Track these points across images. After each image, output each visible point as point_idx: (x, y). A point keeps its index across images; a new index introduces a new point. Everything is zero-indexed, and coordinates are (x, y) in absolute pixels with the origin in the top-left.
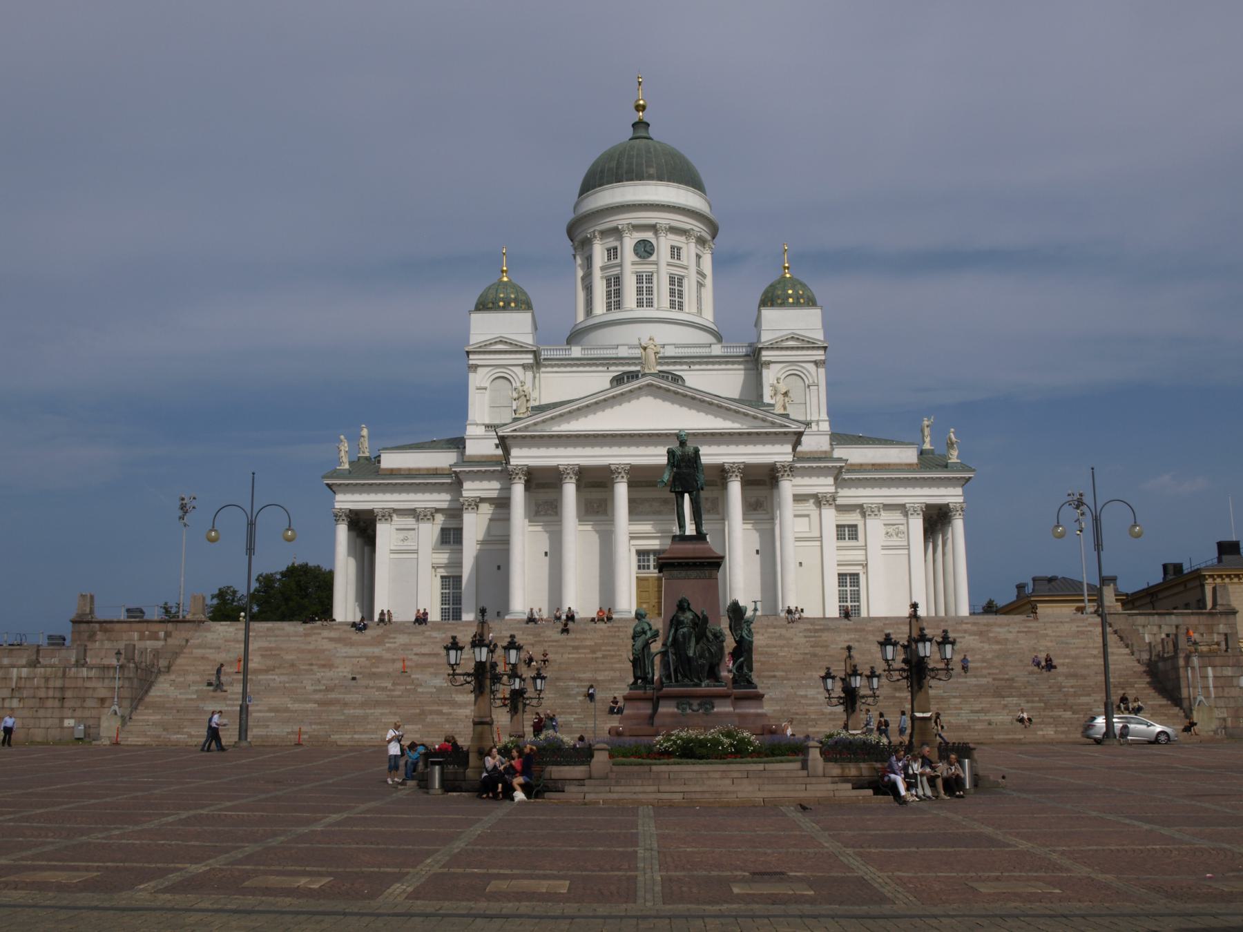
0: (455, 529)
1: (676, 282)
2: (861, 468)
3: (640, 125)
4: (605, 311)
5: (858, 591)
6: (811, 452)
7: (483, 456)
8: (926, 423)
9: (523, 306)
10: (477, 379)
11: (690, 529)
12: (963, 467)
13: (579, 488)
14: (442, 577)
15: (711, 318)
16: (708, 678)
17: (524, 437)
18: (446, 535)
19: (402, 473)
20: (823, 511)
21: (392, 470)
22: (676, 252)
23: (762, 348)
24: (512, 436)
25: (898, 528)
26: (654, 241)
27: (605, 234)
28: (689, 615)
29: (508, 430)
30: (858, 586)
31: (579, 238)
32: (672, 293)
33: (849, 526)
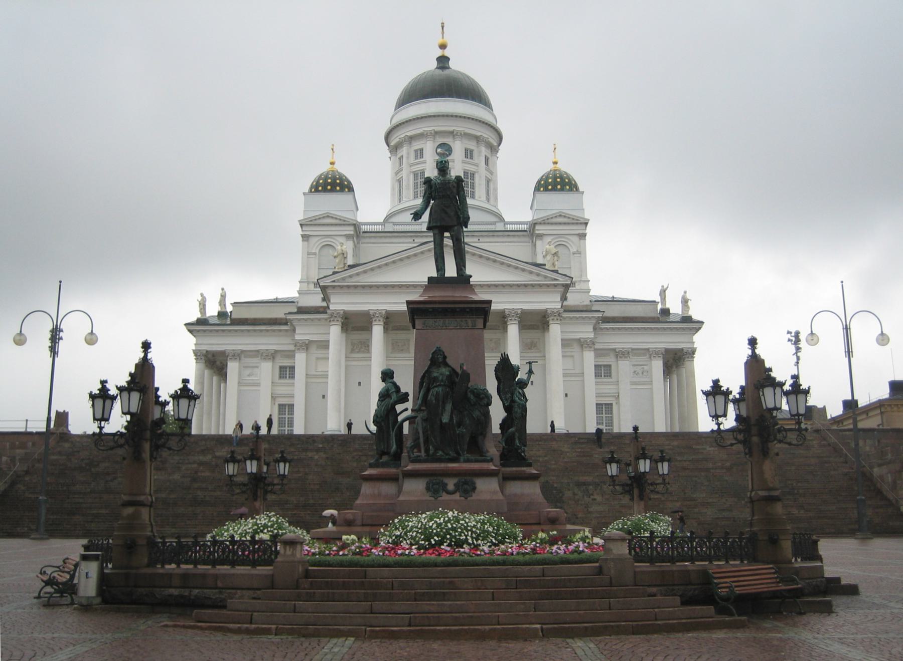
0: (290, 367)
3: (443, 61)
5: (611, 417)
7: (312, 307)
11: (451, 271)
13: (385, 332)
14: (280, 405)
16: (467, 453)
17: (341, 287)
20: (584, 352)
23: (536, 223)
25: (643, 368)
28: (445, 371)
30: (612, 413)
31: (392, 144)
33: (605, 366)
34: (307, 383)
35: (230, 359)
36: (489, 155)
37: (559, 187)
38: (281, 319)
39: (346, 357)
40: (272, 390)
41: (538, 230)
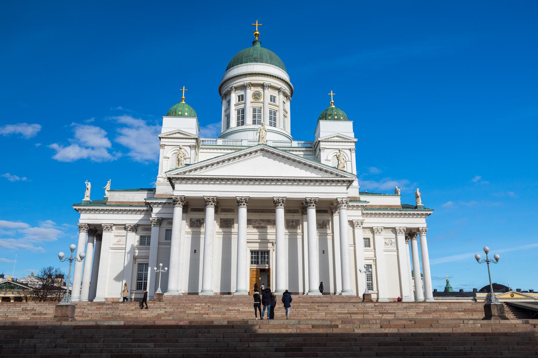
2: (372, 208)
4: (236, 126)
12: (425, 209)
14: (138, 263)
22: (273, 99)
24: (175, 178)
27: (236, 88)
31: (224, 92)
32: (271, 118)
34: (158, 248)
35: (105, 230)
41: (322, 145)
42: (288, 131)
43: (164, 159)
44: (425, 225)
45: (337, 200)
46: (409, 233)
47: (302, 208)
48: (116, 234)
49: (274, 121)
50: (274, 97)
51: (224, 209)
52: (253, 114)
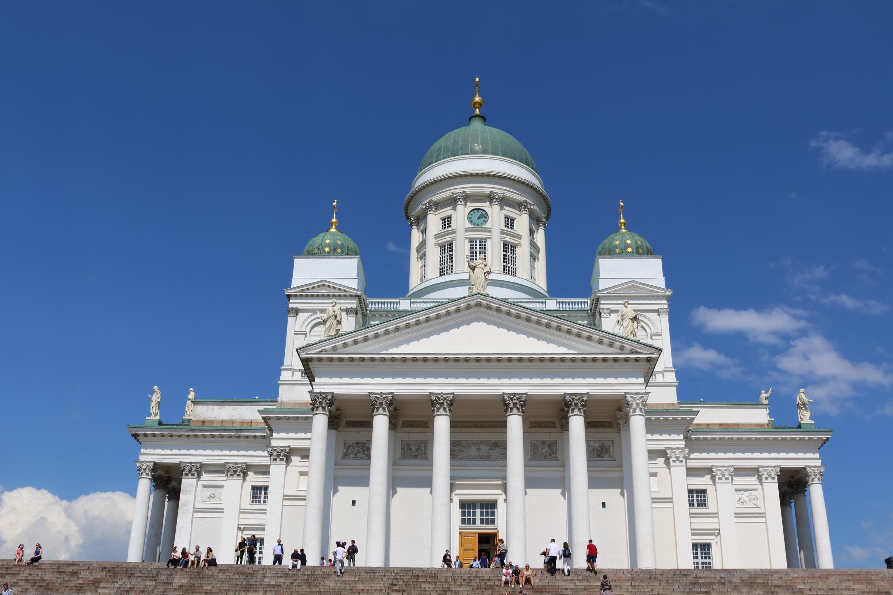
1: (509, 251)
2: (708, 428)
4: (439, 276)
6: (656, 405)
7: (296, 403)
8: (764, 395)
9: (349, 253)
10: (294, 324)
13: (393, 426)
15: (545, 287)
17: (331, 360)
18: (257, 493)
19: (214, 425)
21: (204, 422)
22: (509, 221)
26: (488, 210)
27: (438, 205)
29: (311, 352)
32: (505, 259)
36: (534, 228)
37: (629, 250)
38: (257, 423)
39: (335, 465)
40: (239, 518)
42: (541, 283)
43: (297, 336)
44: (818, 463)
45: (625, 397)
46: (790, 481)
47: (561, 417)
48: (206, 483)
49: (512, 263)
50: (511, 220)
51: (407, 421)
52: (471, 253)
